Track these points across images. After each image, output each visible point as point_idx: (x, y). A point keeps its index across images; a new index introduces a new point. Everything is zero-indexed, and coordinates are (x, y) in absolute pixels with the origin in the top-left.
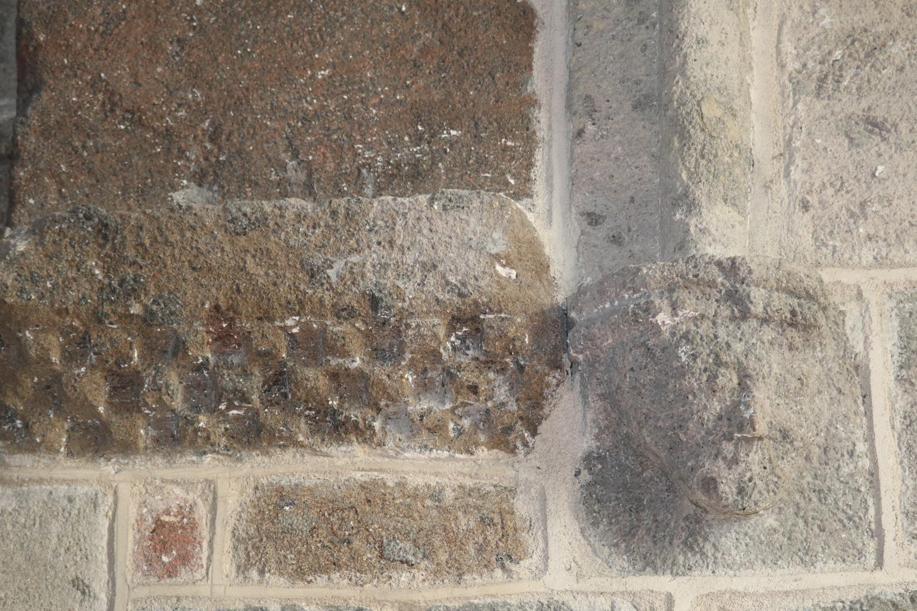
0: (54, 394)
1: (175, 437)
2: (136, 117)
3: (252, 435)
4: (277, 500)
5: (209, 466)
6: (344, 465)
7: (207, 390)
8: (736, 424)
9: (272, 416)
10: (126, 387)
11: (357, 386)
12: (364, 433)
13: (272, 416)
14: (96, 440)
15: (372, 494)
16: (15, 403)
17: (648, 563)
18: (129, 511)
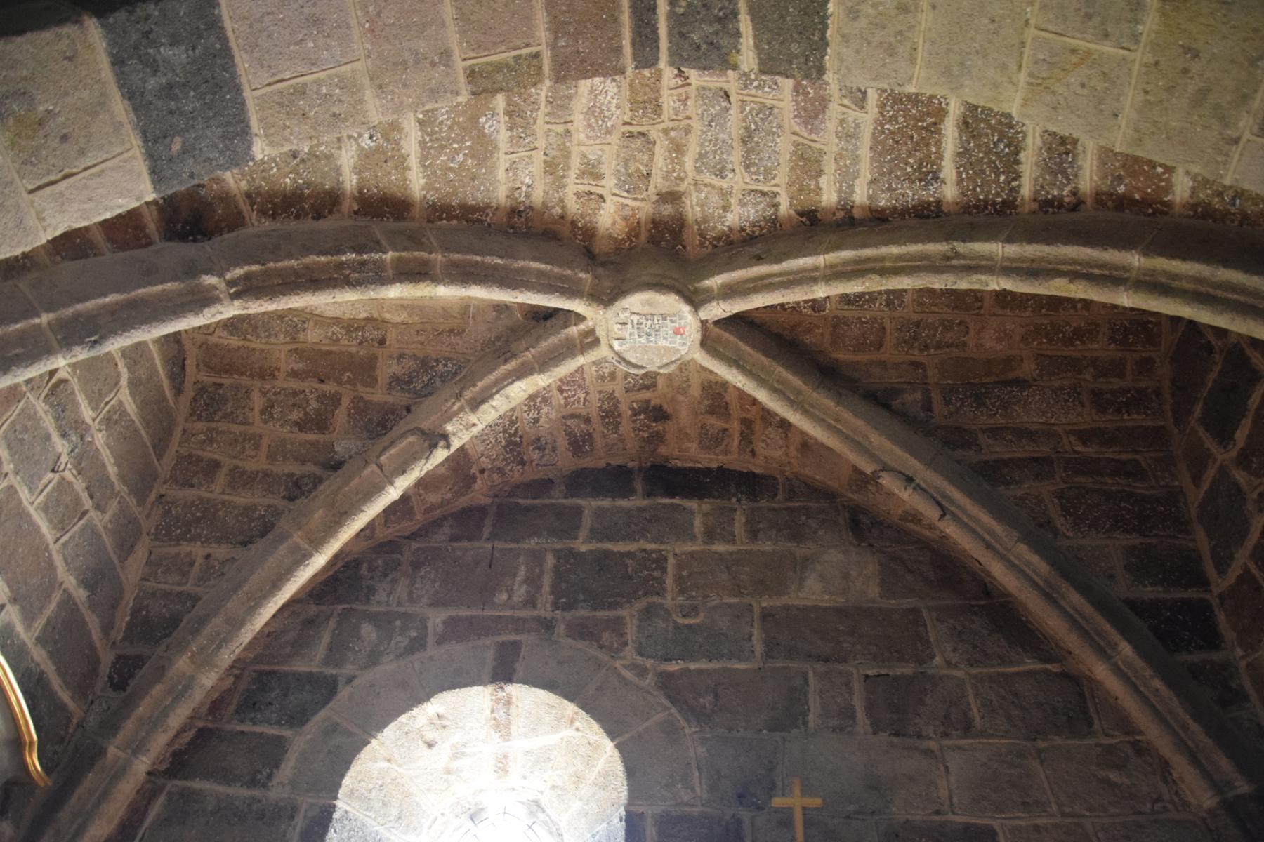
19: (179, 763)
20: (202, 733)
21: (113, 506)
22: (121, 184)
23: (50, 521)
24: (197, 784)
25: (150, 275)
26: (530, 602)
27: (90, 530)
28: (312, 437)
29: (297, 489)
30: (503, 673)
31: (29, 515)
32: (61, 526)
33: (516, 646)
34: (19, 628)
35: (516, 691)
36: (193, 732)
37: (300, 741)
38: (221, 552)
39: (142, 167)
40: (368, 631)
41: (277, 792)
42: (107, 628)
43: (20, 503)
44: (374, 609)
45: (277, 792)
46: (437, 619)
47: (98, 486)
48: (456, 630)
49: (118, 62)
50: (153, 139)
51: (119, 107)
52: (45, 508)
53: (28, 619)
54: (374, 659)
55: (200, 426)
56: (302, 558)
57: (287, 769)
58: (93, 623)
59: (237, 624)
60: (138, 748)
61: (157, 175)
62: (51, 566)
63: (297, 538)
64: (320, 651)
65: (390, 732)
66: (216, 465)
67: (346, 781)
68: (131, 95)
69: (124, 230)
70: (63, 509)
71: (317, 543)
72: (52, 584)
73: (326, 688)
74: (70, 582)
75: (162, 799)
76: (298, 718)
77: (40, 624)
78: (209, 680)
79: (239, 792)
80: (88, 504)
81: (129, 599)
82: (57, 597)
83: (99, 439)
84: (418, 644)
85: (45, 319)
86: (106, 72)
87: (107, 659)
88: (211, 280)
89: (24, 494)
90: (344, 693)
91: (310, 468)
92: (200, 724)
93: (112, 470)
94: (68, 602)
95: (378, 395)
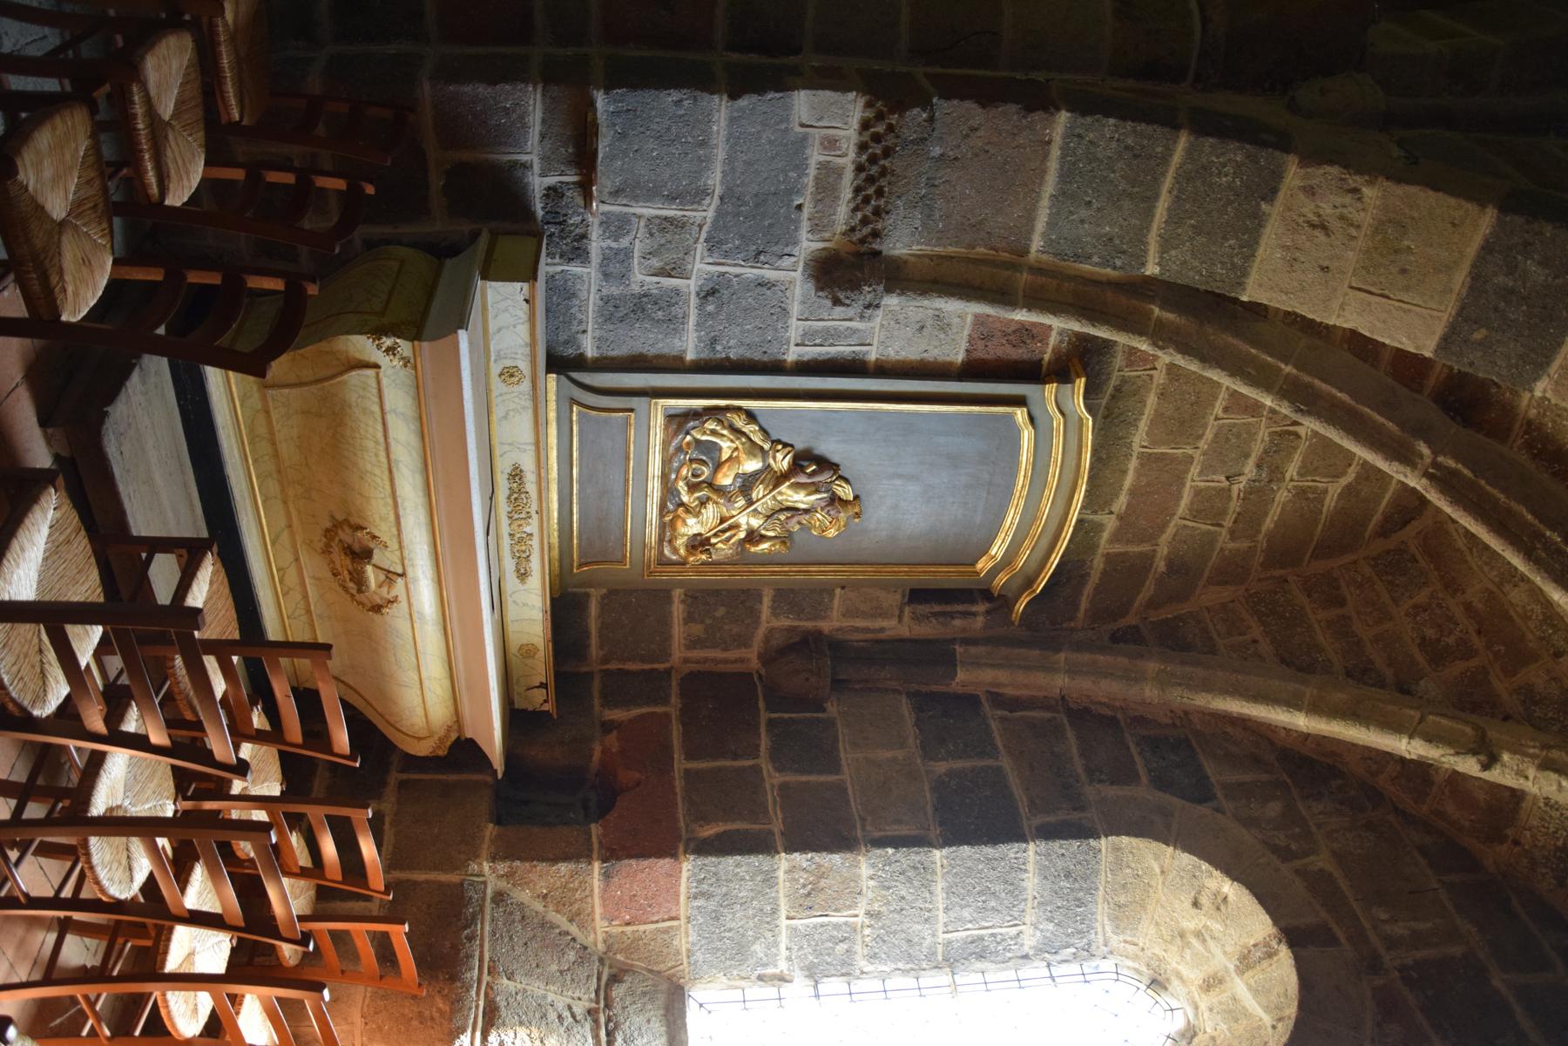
0: (880, 117)
1: (862, 147)
2: (967, 136)
3: (859, 168)
4: (839, 172)
5: (852, 155)
6: (847, 193)
7: (873, 160)
8: (837, 302)
9: (863, 175)
10: (877, 138)
11: (867, 200)
12: (854, 198)
13: (863, 175)
14: (865, 125)
15: (838, 198)
16: (879, 104)
17: (806, 264)
18: (842, 133)
19: (1083, 715)
20: (1113, 721)
21: (1244, 545)
22: (1412, 327)
23: (1192, 503)
24: (1070, 734)
25: (1387, 408)
26: (1392, 943)
27: (1211, 539)
28: (1420, 658)
29: (1361, 673)
30: (1294, 936)
31: (1184, 485)
32: (1196, 514)
33: (1333, 941)
34: (1105, 535)
35: (1285, 955)
36: (1110, 713)
37: (1143, 791)
38: (1265, 647)
39: (1439, 329)
40: (1274, 809)
41: (1090, 791)
42: (1152, 604)
43: (1187, 471)
44: (1301, 806)
45: (1090, 791)
46: (1322, 861)
47: (1248, 521)
48: (1319, 884)
49: (1487, 248)
50: (1465, 318)
51: (1460, 278)
52: (1198, 492)
53: (1116, 538)
54: (1249, 822)
55: (1368, 571)
56: (1293, 703)
57: (1112, 791)
58: (1148, 590)
59: (1207, 687)
60: (1073, 671)
61: (1445, 343)
62: (1162, 527)
63: (1309, 692)
64: (1235, 777)
65: (1186, 859)
66: (1342, 603)
67: (1125, 840)
68: (1477, 279)
69: (1408, 367)
70: (1209, 506)
71: (1315, 709)
72: (1152, 538)
73: (1201, 793)
74: (1163, 550)
75: (1048, 715)
76: (1161, 782)
77: (1118, 548)
78: (1150, 692)
79: (1079, 765)
80: (1228, 522)
81: (1185, 609)
82: (1145, 548)
83: (1282, 496)
84: (1285, 854)
85: (1288, 369)
86: (1472, 250)
87: (1131, 620)
88: (1425, 450)
89: (1194, 470)
90: (1204, 809)
91: (1389, 673)
92: (1119, 716)
93: (1268, 524)
94: (1148, 558)
95: (1501, 687)
